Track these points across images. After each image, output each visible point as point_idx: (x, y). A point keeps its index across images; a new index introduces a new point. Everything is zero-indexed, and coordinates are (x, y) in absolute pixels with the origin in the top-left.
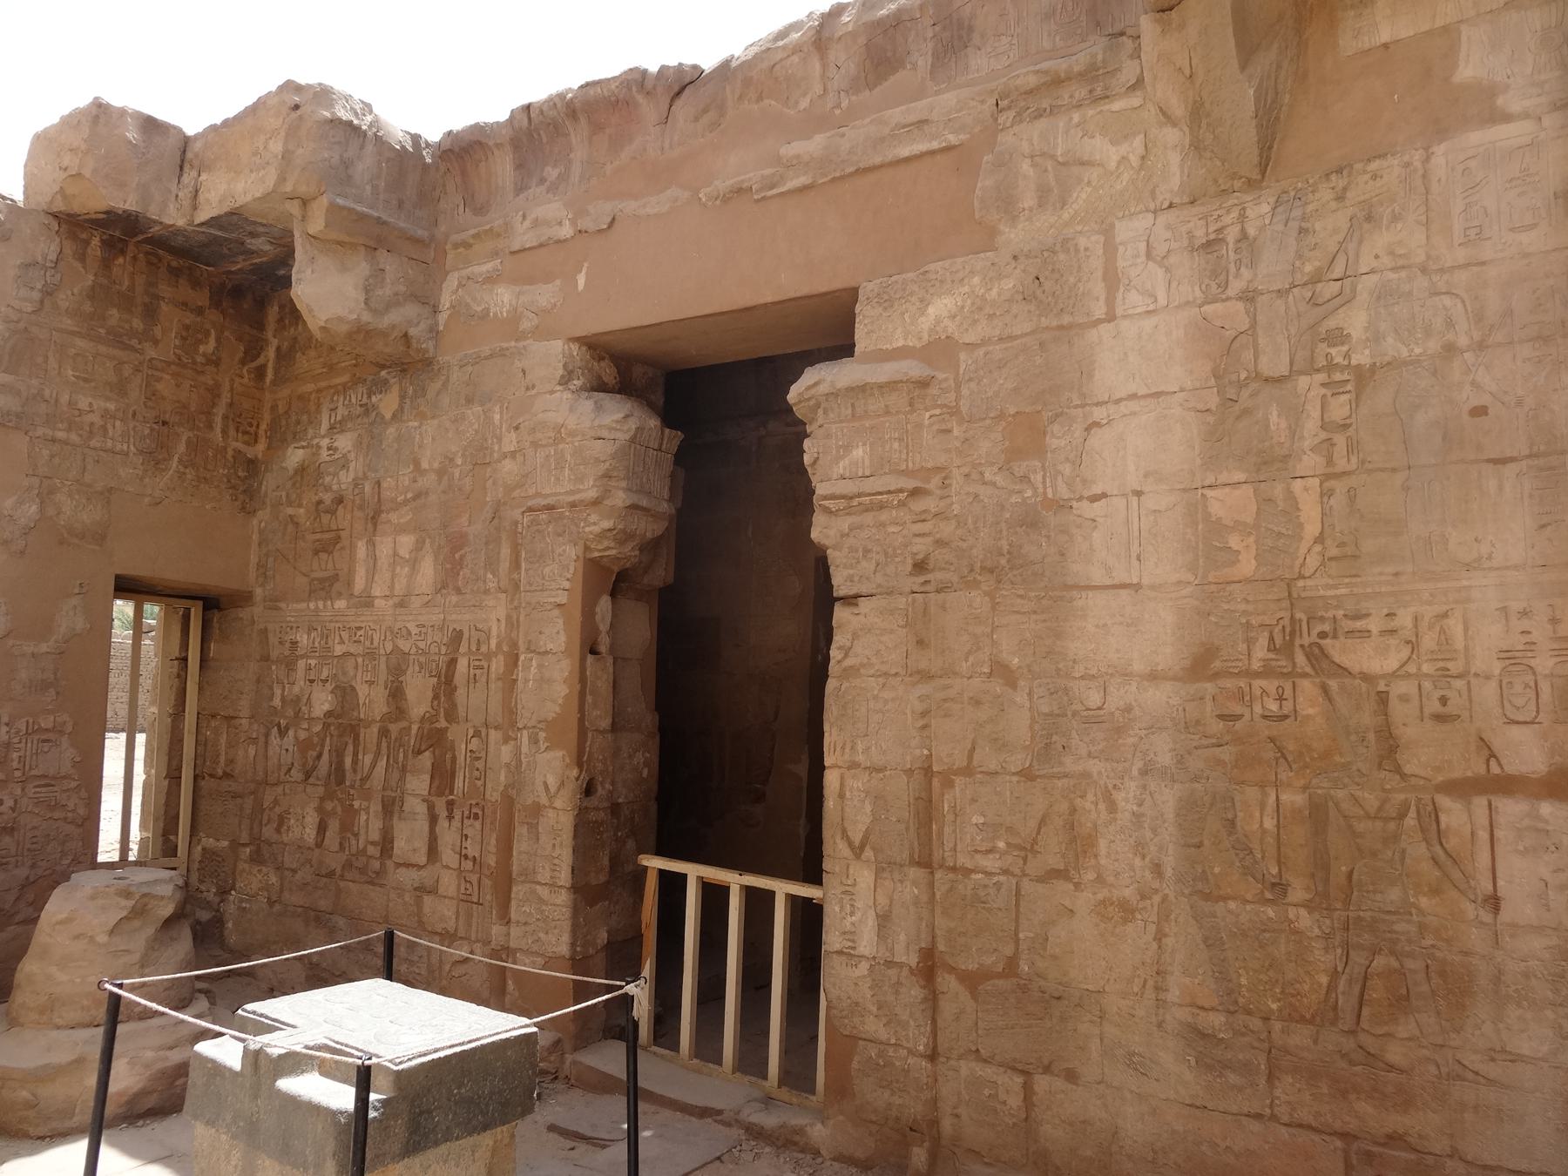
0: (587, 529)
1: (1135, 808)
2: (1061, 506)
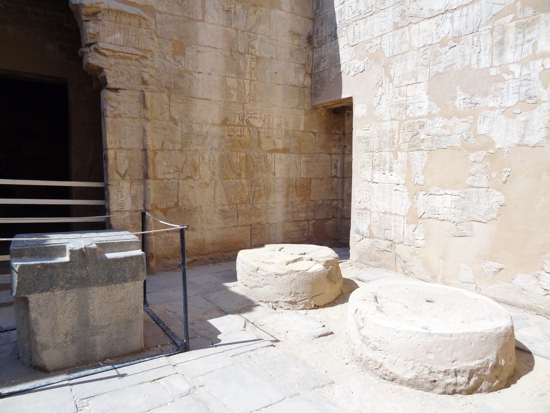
1: (209, 158)
2: (190, 73)
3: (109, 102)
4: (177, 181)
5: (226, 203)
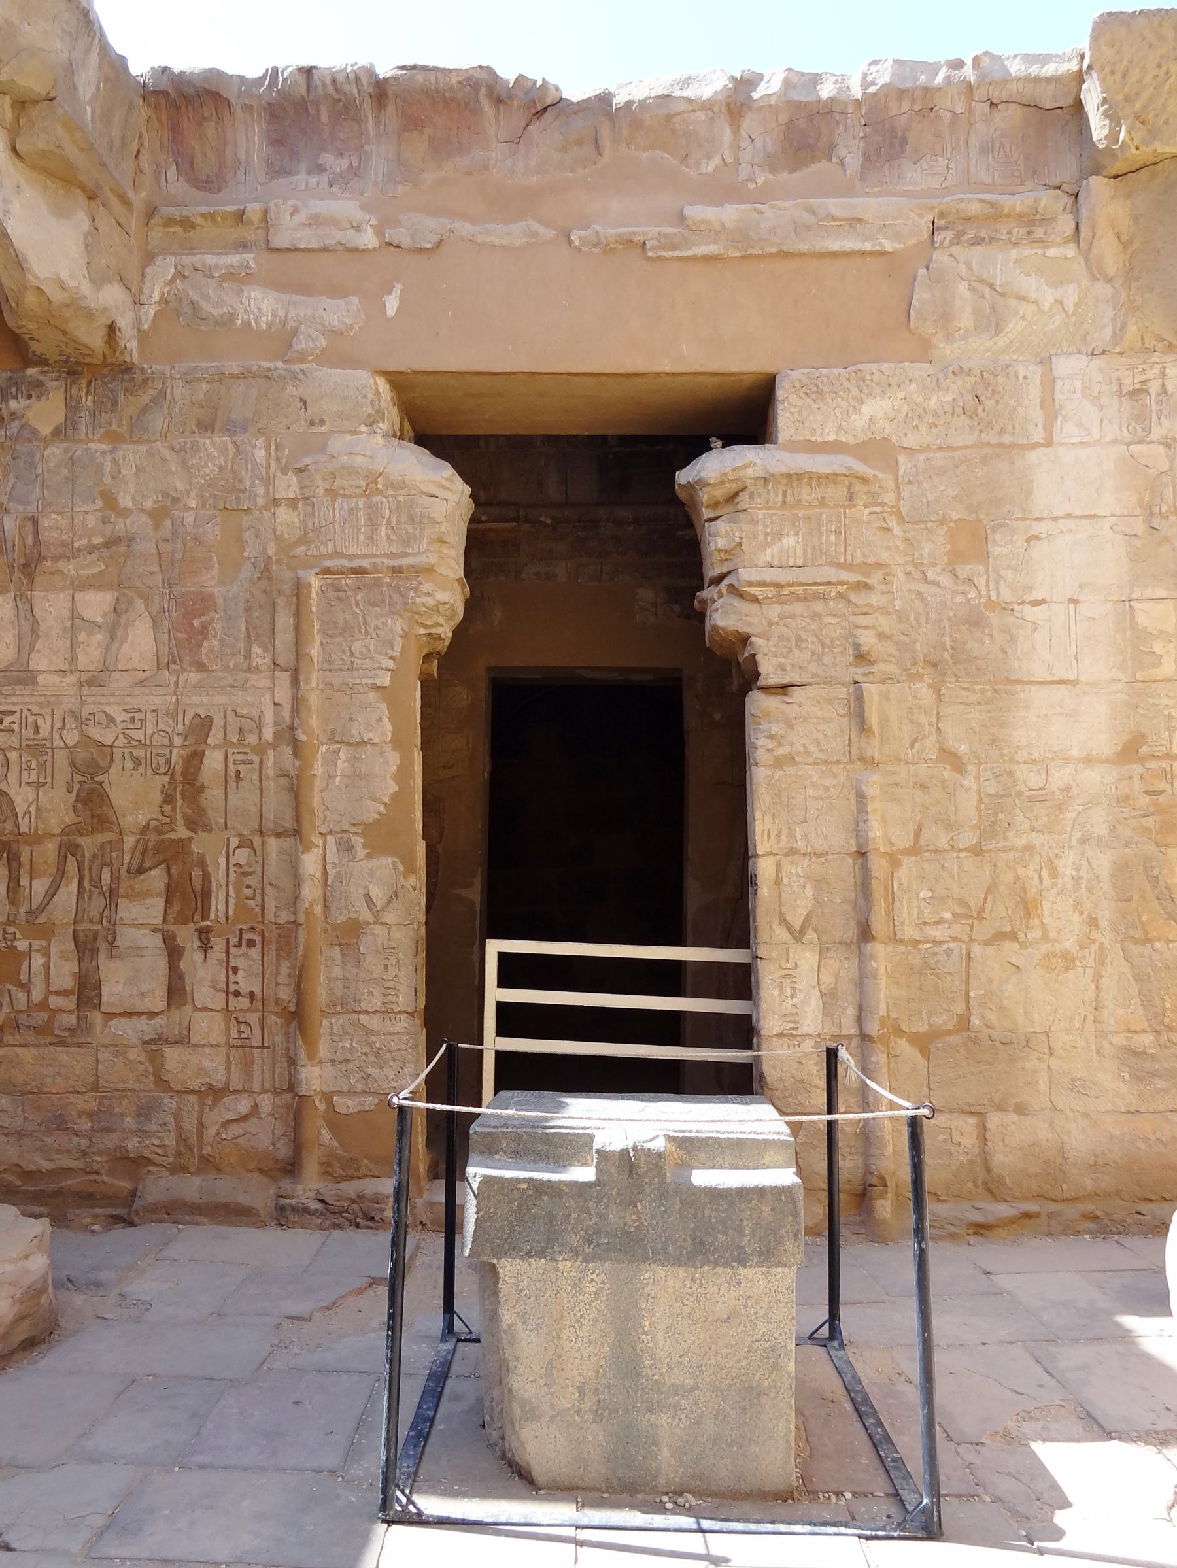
0: (418, 600)
1: (1074, 873)
3: (765, 726)
4: (964, 947)
5: (1145, 1025)
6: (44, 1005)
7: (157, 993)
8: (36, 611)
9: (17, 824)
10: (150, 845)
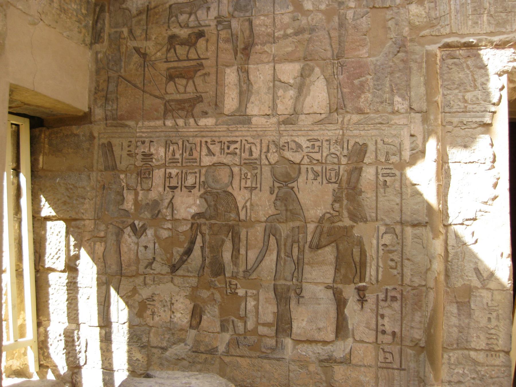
6: (255, 331)
7: (329, 329)
8: (251, 77)
9: (238, 214)
10: (325, 229)
